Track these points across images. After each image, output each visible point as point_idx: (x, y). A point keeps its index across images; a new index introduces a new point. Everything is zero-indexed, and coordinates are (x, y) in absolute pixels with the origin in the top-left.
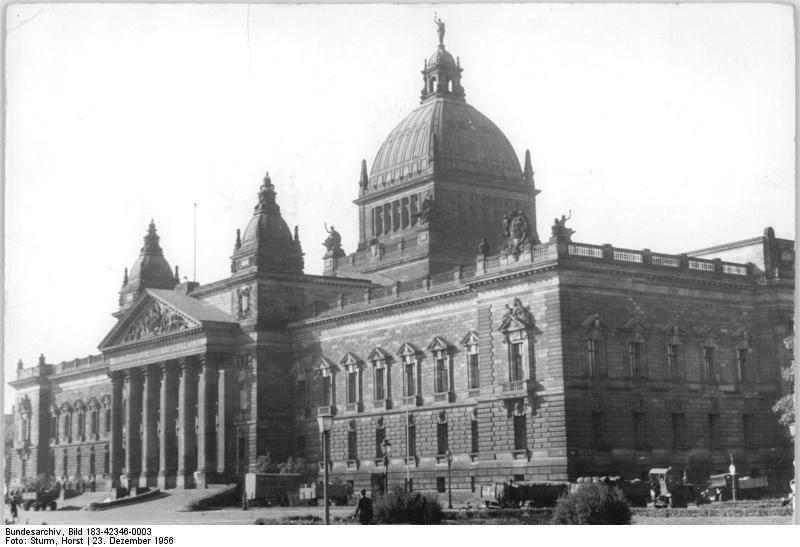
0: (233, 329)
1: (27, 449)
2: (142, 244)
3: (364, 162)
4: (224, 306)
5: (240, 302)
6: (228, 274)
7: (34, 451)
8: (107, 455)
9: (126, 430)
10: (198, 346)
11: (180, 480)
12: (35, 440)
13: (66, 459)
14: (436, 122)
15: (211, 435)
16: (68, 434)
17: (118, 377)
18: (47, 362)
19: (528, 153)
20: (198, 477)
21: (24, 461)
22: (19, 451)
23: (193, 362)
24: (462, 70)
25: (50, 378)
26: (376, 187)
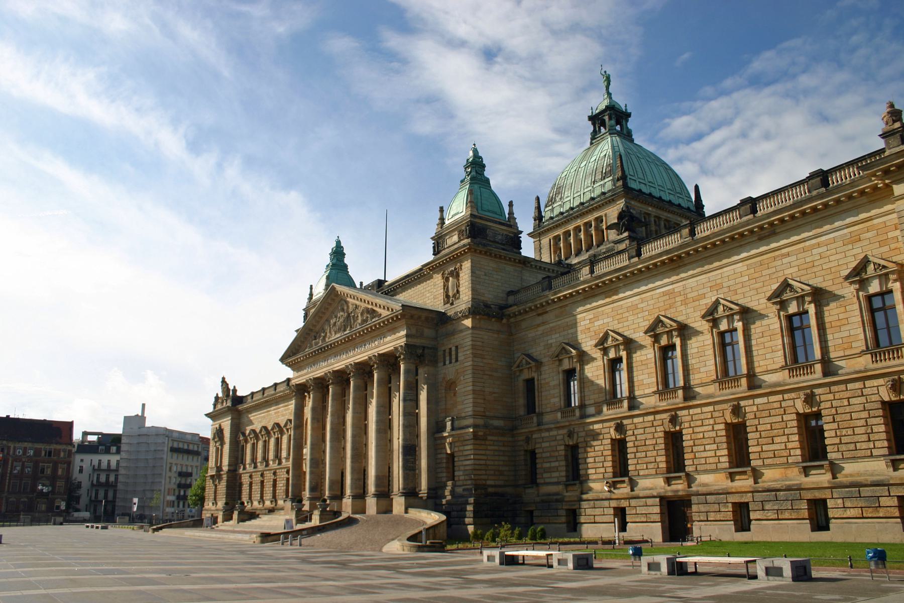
0: (440, 320)
1: (217, 477)
2: (327, 260)
3: (538, 199)
4: (428, 295)
5: (446, 287)
6: (431, 258)
7: (225, 477)
8: (288, 479)
9: (307, 451)
10: (395, 341)
11: (371, 503)
12: (225, 468)
13: (251, 484)
14: (617, 149)
15: (410, 450)
16: (254, 460)
17: (301, 391)
18: (239, 394)
19: (697, 188)
20: (399, 504)
21: (216, 486)
22: (212, 477)
23: (389, 361)
24: (629, 115)
25: (240, 407)
26: (552, 218)
